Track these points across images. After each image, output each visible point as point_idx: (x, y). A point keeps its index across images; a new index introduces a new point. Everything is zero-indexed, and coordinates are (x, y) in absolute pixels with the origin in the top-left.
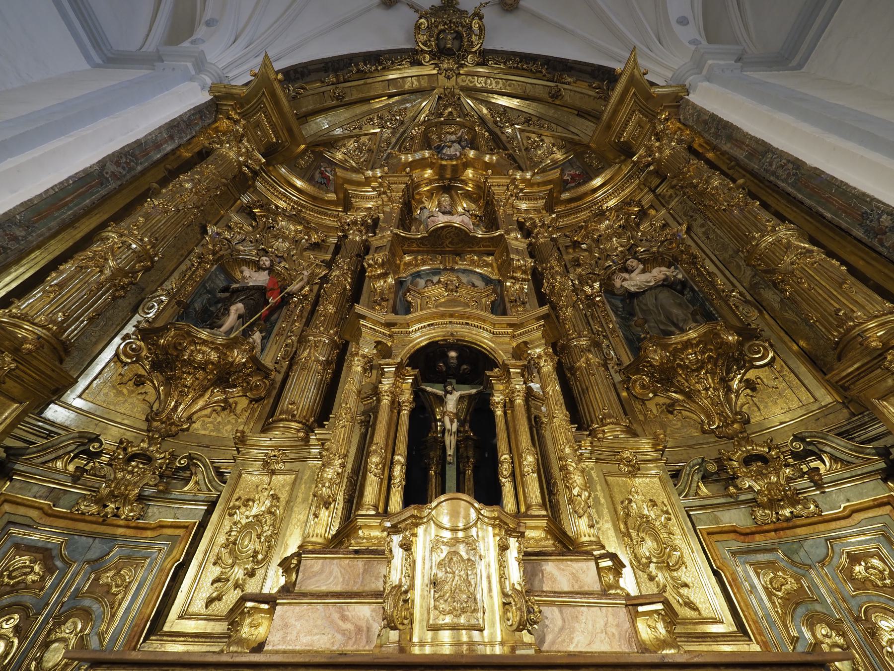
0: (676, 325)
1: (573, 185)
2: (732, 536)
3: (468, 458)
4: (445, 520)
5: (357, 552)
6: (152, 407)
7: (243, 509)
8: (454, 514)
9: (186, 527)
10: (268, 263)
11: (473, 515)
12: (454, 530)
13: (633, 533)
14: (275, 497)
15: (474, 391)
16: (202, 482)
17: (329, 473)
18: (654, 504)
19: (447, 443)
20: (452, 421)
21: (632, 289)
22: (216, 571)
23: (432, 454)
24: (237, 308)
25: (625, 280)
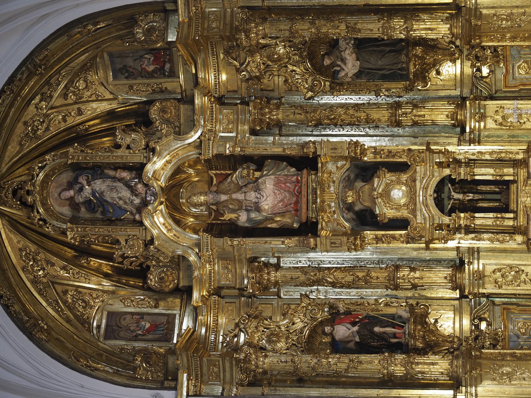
0: (399, 63)
1: (168, 66)
2: (507, 77)
3: (471, 188)
4: (526, 199)
5: (528, 223)
6: (446, 353)
7: (499, 283)
8: (524, 197)
9: (504, 309)
10: (329, 328)
11: (524, 192)
12: (527, 197)
13: (509, 124)
14: (494, 272)
15: (450, 185)
16: (484, 311)
17: (501, 239)
18: (497, 111)
19: (477, 198)
20: (468, 196)
21: (356, 71)
22: (522, 284)
23: (469, 205)
24: (377, 329)
25: (346, 74)
